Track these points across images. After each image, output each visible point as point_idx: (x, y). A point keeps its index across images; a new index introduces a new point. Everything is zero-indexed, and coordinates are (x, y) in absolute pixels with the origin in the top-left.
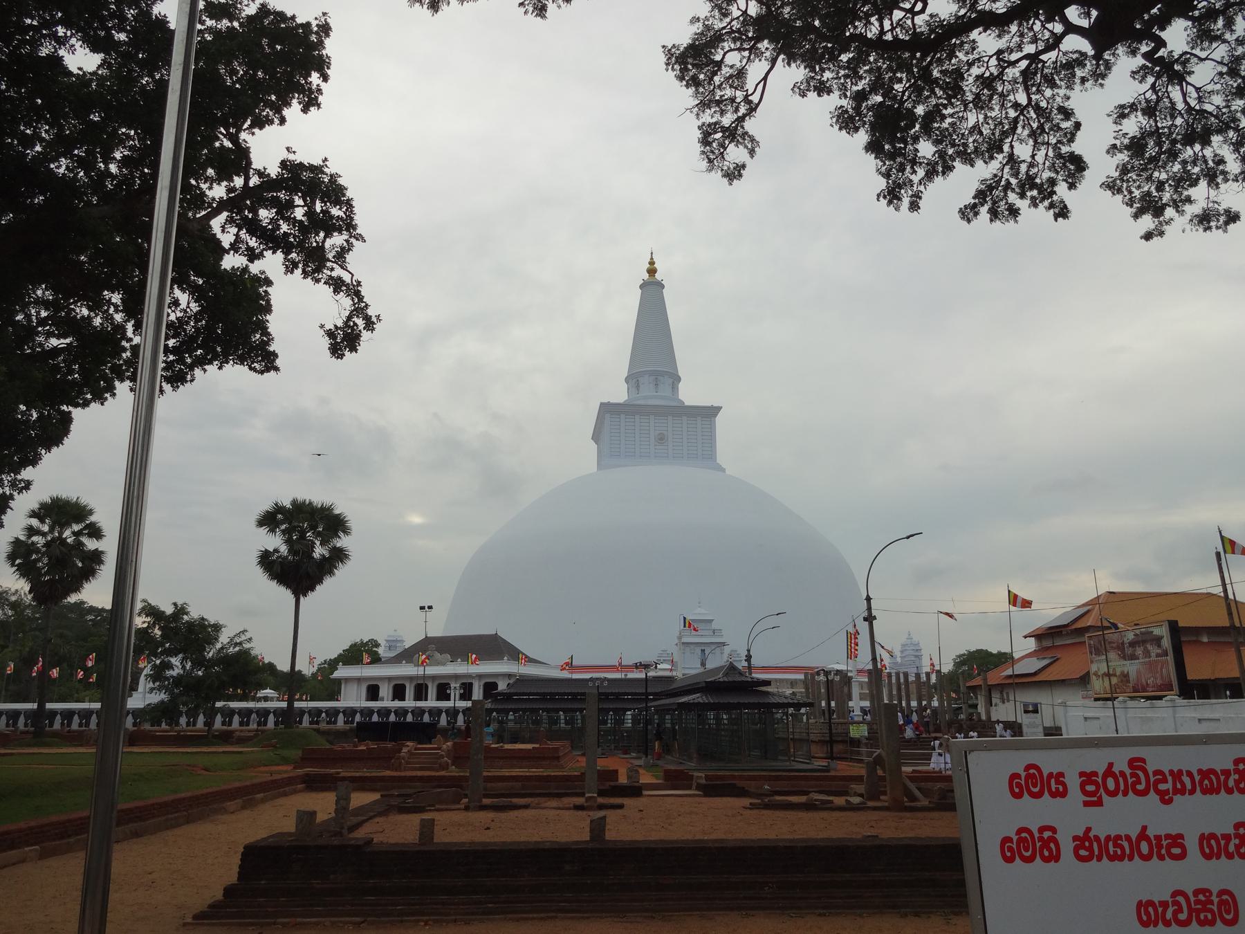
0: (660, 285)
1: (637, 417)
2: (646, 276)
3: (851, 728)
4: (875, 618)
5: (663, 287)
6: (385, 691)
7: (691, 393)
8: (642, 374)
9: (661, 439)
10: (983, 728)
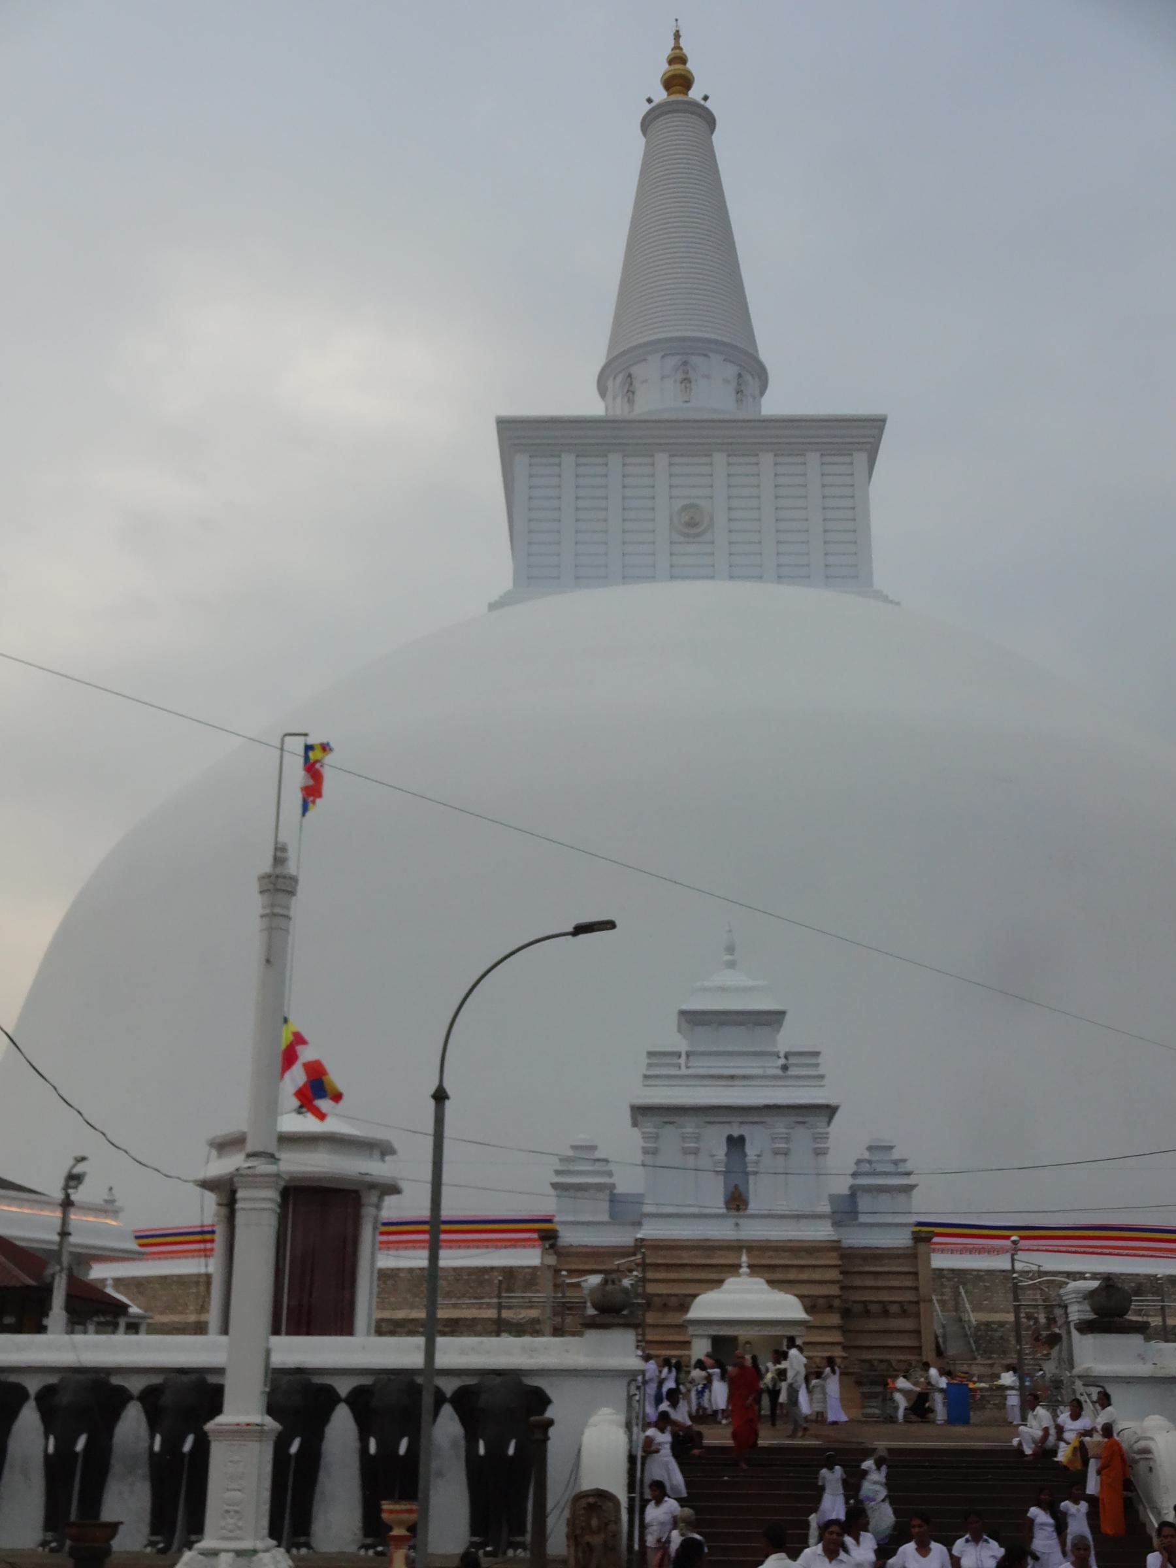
1: (615, 459)
2: (661, 95)
5: (710, 121)
8: (640, 353)
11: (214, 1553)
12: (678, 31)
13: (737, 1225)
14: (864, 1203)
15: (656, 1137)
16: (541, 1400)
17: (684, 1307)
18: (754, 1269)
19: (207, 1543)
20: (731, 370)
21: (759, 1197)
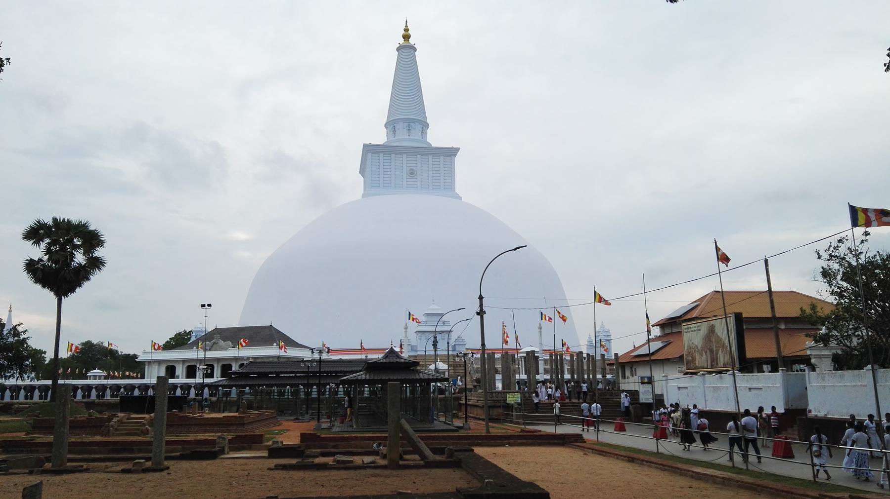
1: (393, 155)
2: (402, 41)
3: (508, 396)
4: (485, 313)
5: (415, 50)
6: (180, 370)
7: (436, 138)
9: (412, 173)
10: (611, 396)
14: (457, 346)
15: (421, 336)
20: (421, 126)
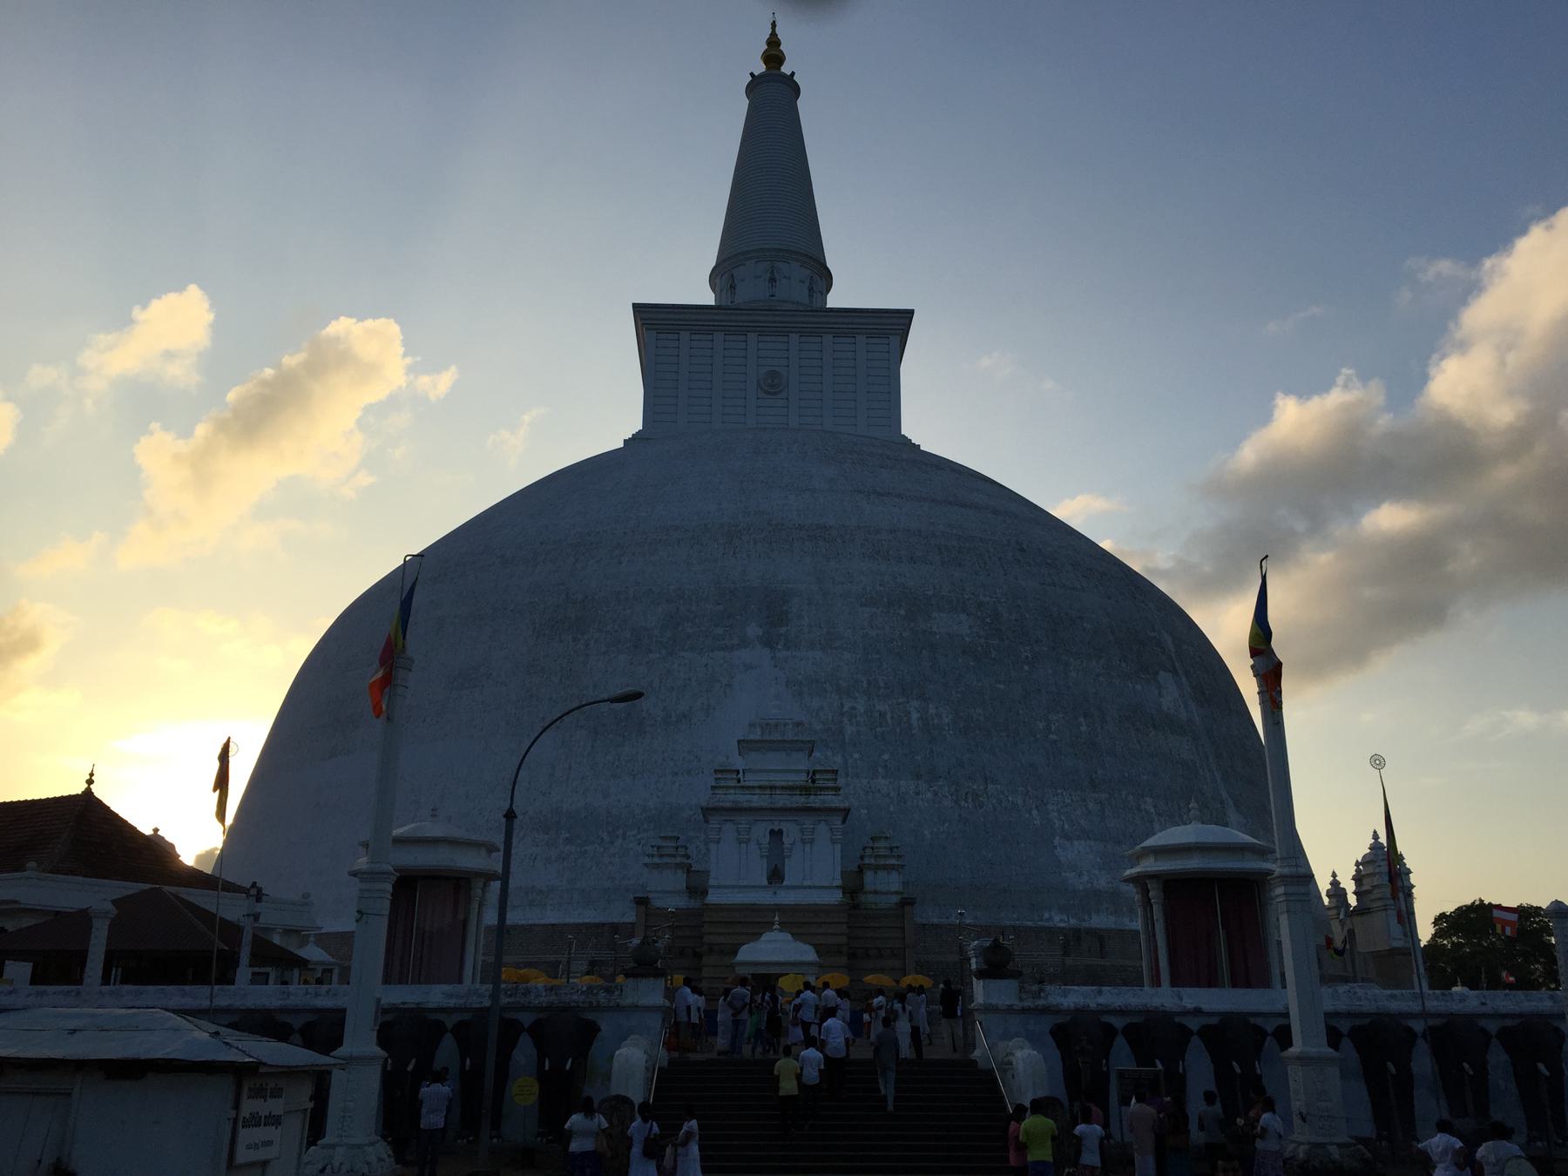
0: (791, 87)
2: (760, 68)
5: (796, 90)
11: (333, 1146)
12: (774, 22)
13: (775, 893)
16: (591, 1030)
17: (735, 953)
18: (784, 926)
19: (327, 1140)
21: (792, 874)
